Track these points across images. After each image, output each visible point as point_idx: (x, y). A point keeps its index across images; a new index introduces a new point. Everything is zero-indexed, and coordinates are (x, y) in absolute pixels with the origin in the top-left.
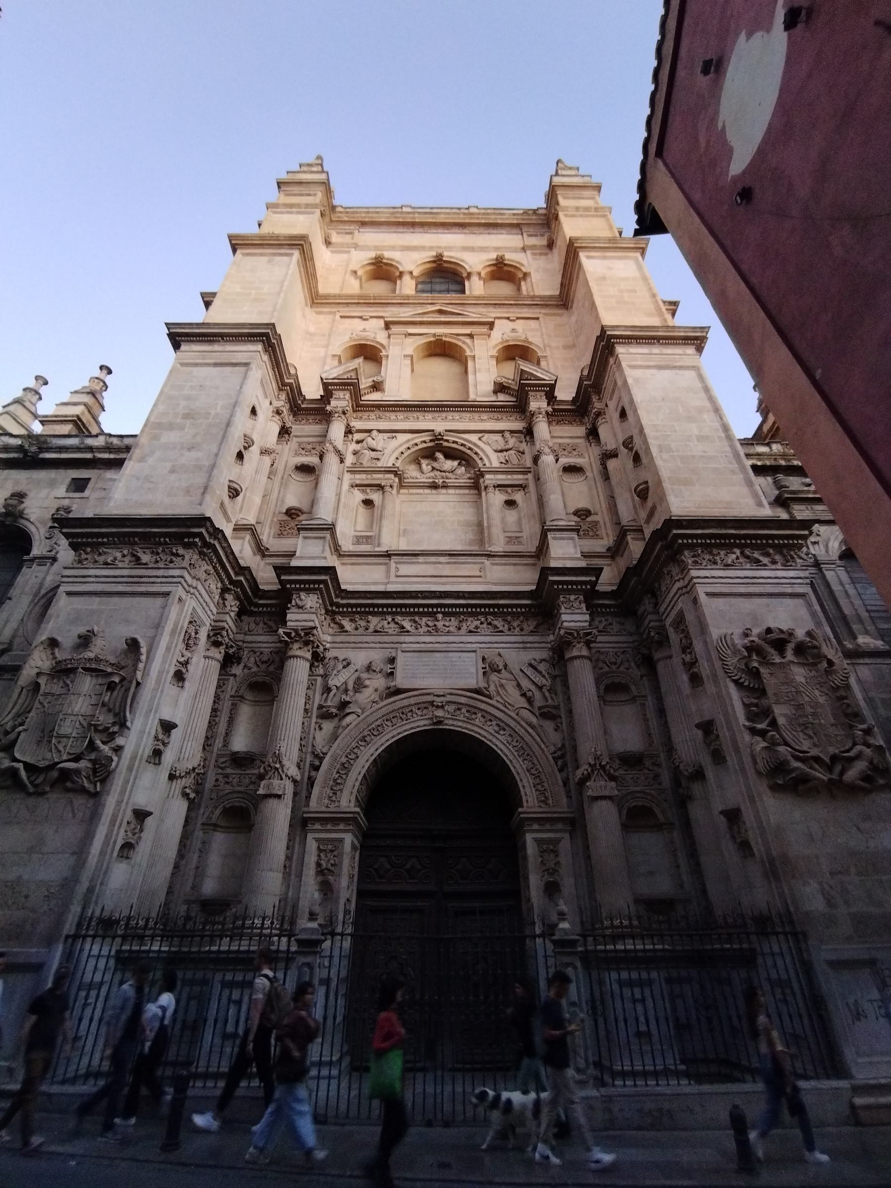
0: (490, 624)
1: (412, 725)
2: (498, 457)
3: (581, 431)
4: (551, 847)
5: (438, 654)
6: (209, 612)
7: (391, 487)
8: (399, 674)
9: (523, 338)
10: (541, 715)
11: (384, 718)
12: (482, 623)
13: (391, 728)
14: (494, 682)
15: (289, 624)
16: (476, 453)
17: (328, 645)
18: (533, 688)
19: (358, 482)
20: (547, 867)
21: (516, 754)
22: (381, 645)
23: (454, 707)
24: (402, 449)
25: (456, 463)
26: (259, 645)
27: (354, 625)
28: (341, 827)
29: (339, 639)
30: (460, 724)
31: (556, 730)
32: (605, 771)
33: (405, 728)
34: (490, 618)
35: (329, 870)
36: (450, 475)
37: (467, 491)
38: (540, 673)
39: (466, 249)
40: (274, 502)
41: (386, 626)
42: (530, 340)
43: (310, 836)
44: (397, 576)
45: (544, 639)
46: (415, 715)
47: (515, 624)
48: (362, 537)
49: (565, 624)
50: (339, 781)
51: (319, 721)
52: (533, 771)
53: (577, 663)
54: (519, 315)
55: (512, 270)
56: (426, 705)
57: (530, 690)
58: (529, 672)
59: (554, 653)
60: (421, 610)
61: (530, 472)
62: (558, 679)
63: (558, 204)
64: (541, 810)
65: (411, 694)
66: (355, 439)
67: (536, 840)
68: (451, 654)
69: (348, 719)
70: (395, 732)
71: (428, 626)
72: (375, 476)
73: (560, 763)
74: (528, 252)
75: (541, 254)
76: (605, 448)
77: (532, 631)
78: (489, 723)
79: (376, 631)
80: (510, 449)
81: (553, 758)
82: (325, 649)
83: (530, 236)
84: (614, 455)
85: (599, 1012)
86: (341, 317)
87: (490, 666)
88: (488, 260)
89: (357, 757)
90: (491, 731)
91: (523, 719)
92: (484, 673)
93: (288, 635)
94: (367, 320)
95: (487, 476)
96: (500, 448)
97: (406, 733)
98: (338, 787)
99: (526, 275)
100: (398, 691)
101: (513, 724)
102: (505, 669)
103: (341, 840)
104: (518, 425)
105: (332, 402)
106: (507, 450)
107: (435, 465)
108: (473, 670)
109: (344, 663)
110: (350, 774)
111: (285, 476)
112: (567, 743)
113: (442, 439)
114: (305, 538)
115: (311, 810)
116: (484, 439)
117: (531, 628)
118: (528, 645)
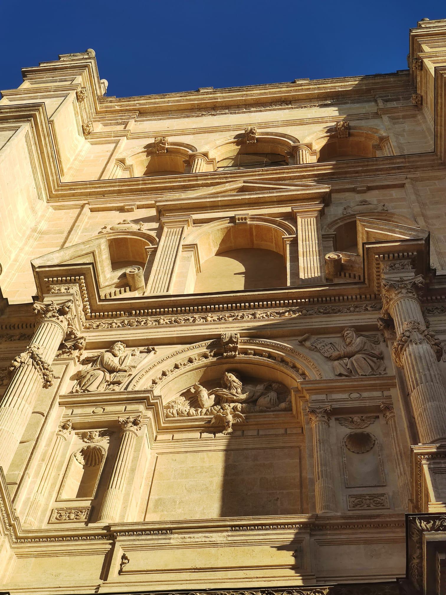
2: (333, 368)
9: (380, 209)
19: (77, 420)
25: (260, 388)
48: (69, 510)
54: (369, 185)
55: (363, 139)
61: (394, 385)
63: (422, 51)
72: (108, 409)
74: (385, 118)
75: (404, 117)
83: (387, 101)
86: (92, 210)
94: (128, 211)
95: (314, 397)
96: (336, 354)
99: (382, 139)
105: (45, 299)
113: (235, 349)
116: (308, 344)
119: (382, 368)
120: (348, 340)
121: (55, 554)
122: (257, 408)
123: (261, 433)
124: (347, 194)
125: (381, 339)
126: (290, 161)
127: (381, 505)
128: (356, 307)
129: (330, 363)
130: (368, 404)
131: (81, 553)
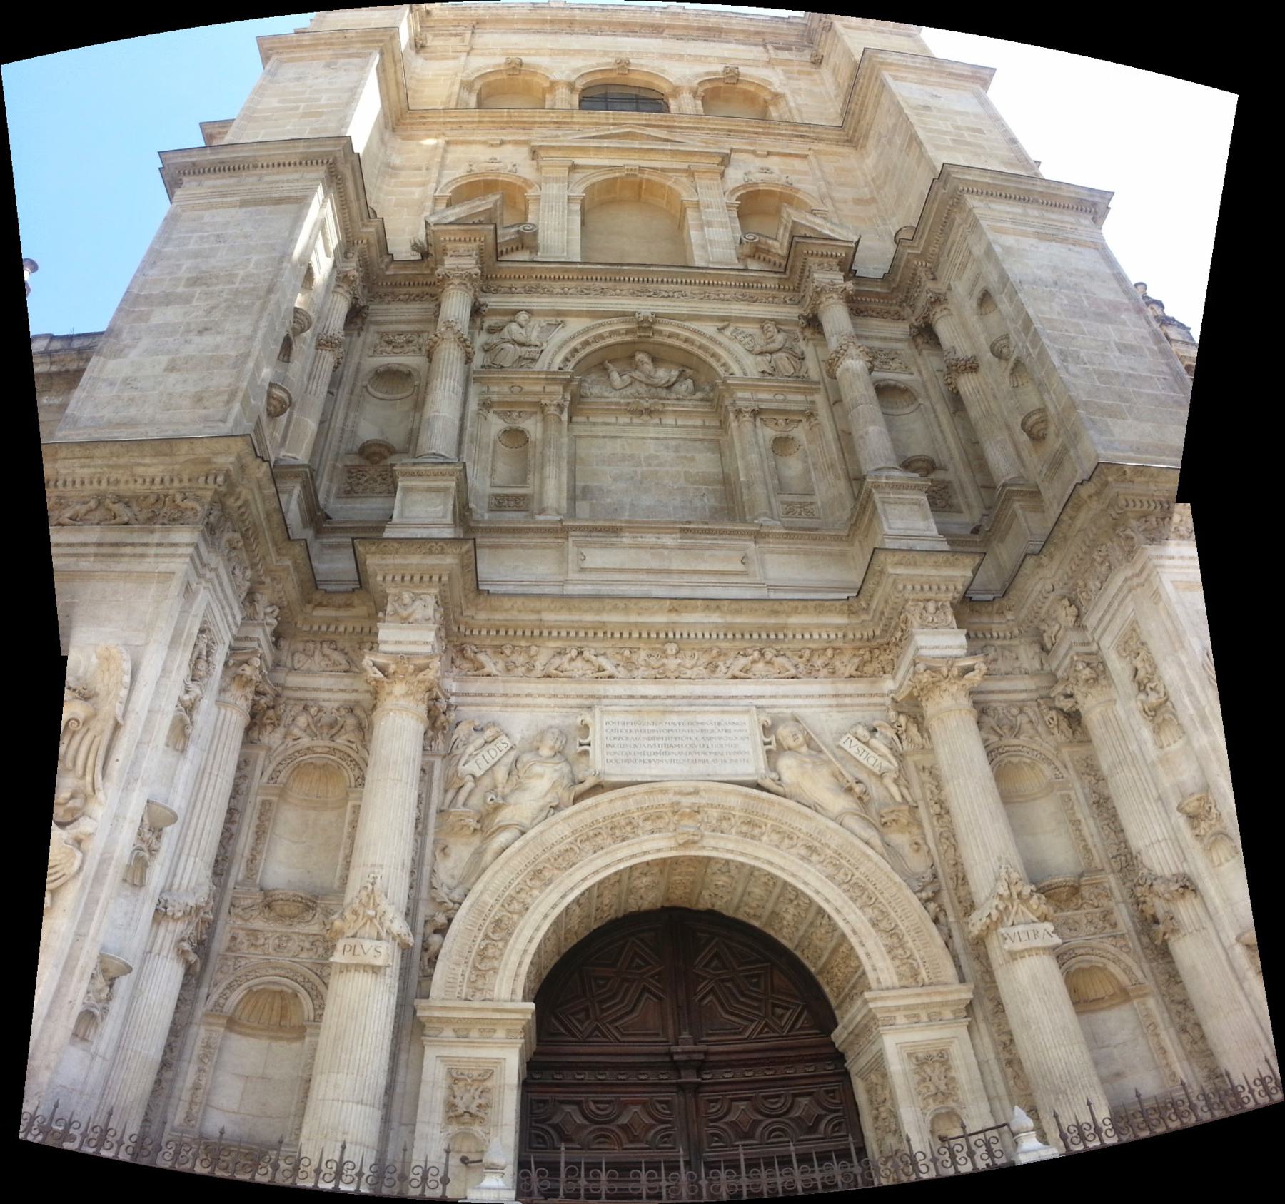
0: (769, 663)
1: (635, 850)
3: (900, 329)
6: (230, 618)
7: (560, 407)
8: (596, 753)
12: (754, 662)
14: (789, 768)
15: (383, 647)
16: (713, 355)
17: (453, 700)
22: (558, 701)
24: (575, 343)
26: (314, 695)
33: (619, 856)
36: (663, 393)
37: (699, 422)
39: (664, 56)
40: (337, 432)
41: (566, 666)
42: (795, 185)
44: (582, 570)
46: (640, 832)
57: (858, 782)
59: (899, 713)
66: (486, 325)
68: (700, 718)
69: (502, 838)
71: (648, 665)
76: (951, 356)
77: (851, 676)
80: (779, 350)
82: (449, 706)
84: (971, 366)
87: (777, 741)
88: (708, 73)
92: (768, 752)
93: (382, 669)
95: (740, 394)
96: (758, 349)
97: (621, 866)
102: (808, 746)
104: (791, 313)
106: (771, 353)
107: (637, 374)
108: (746, 746)
111: (357, 390)
114: (408, 490)
116: (728, 332)
117: (851, 670)
118: (847, 701)
119: (803, 370)
120: (769, 334)
121: (509, 546)
122: (674, 396)
123: (680, 422)
124: (745, 156)
125: (801, 337)
126: (672, 102)
127: (810, 514)
128: (774, 297)
129: (751, 357)
130: (793, 407)
131: (535, 547)
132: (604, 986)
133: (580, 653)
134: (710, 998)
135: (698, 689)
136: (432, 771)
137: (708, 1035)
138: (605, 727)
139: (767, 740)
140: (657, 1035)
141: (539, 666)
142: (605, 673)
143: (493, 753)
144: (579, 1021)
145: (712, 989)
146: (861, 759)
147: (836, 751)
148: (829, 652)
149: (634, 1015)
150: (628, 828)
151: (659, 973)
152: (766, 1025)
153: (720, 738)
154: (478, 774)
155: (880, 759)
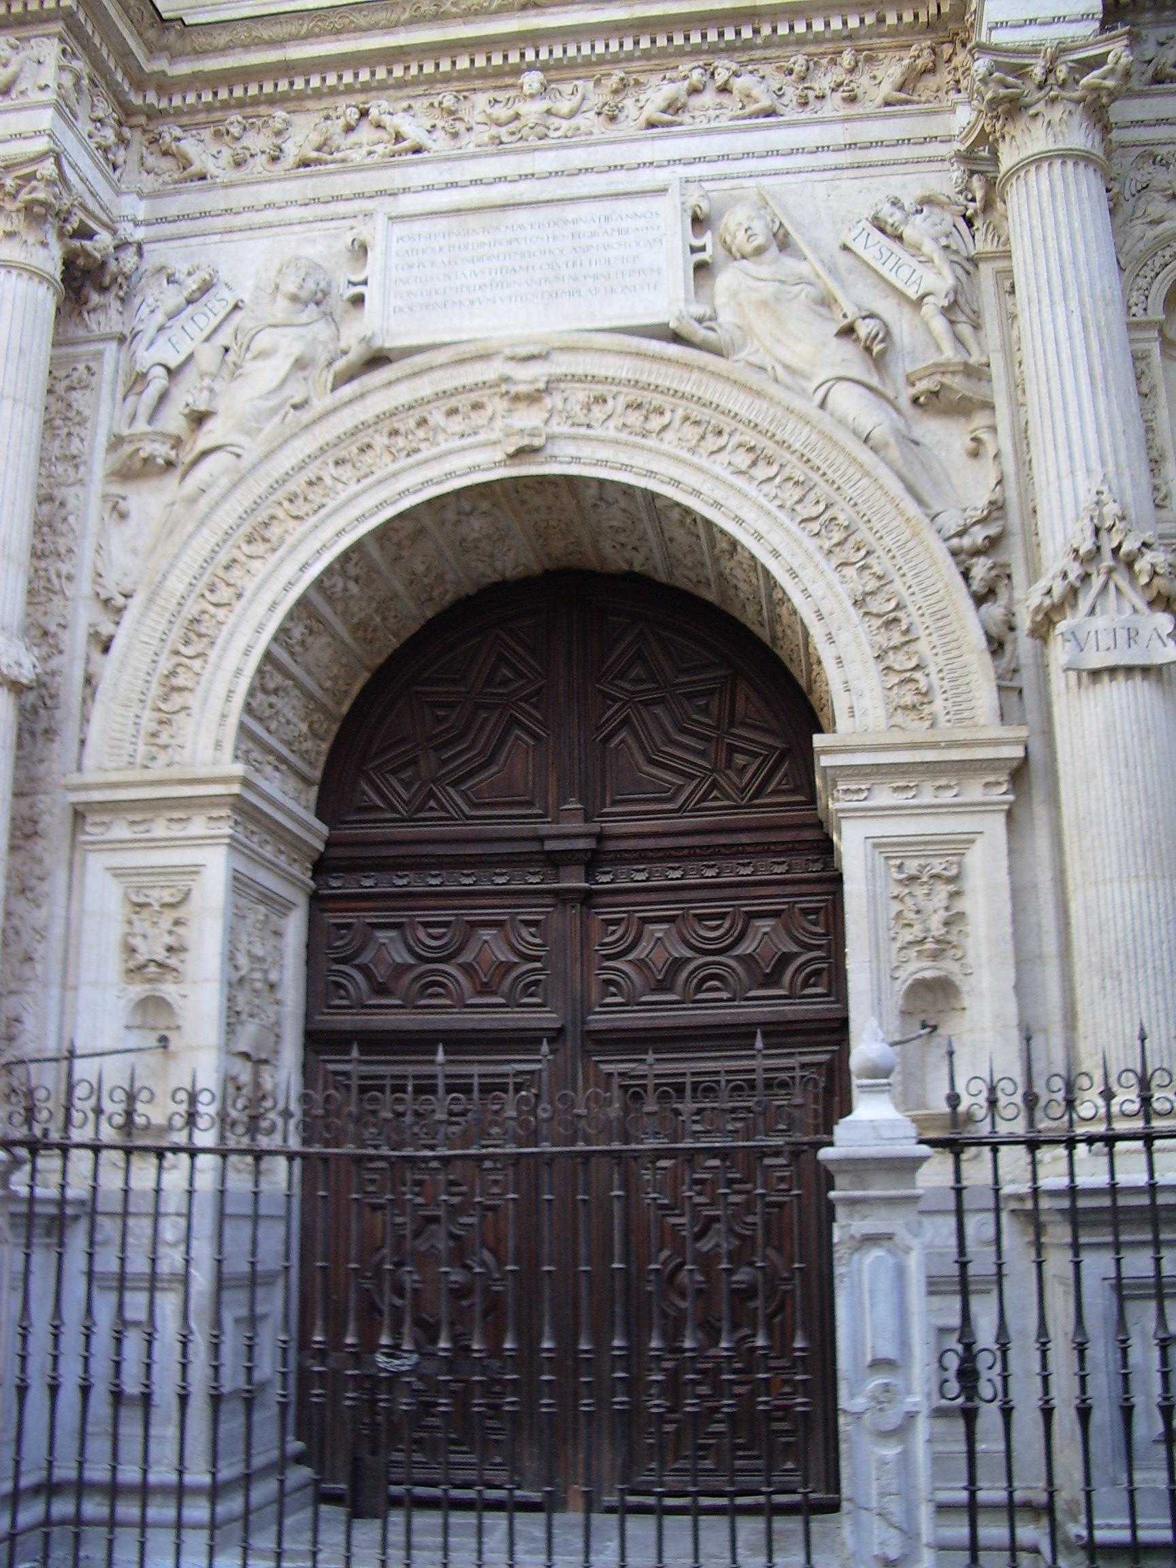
0: (724, 89)
4: (937, 866)
5: (523, 216)
10: (915, 401)
11: (330, 458)
12: (695, 91)
13: (354, 488)
17: (140, 234)
18: (887, 308)
20: (916, 932)
21: (811, 544)
23: (580, 394)
27: (227, 154)
28: (198, 826)
29: (172, 206)
30: (603, 453)
31: (975, 454)
32: (1133, 577)
34: (724, 68)
35: (160, 965)
38: (915, 251)
41: (339, 140)
43: (97, 864)
45: (933, 126)
47: (823, 82)
49: (1001, 37)
50: (179, 681)
51: (116, 489)
52: (874, 605)
53: (1040, 181)
56: (474, 397)
57: (871, 316)
58: (874, 248)
60: (463, 63)
62: (986, 270)
64: (897, 737)
65: (419, 360)
67: (878, 845)
68: (571, 211)
70: (367, 502)
73: (980, 568)
78: (712, 442)
79: (305, 164)
81: (954, 553)
85: (986, 1390)
89: (239, 596)
90: (717, 469)
91: (841, 422)
92: (701, 267)
98: (177, 700)
100: (377, 360)
101: (798, 436)
103: (194, 871)
109: (192, 284)
110: (213, 654)
112: (1012, 494)
115: (90, 777)
117: (887, 89)
118: (875, 155)
132: (445, 719)
133: (364, 114)
134: (623, 734)
135: (577, 157)
136: (102, 368)
137: (615, 803)
138: (395, 247)
139: (697, 243)
140: (530, 804)
141: (292, 151)
142: (405, 144)
143: (201, 320)
144: (401, 781)
145: (626, 722)
146: (884, 271)
147: (843, 259)
148: (847, 59)
149: (494, 769)
150: (421, 433)
151: (537, 692)
152: (714, 785)
153: (606, 247)
154: (173, 365)
155: (921, 269)
